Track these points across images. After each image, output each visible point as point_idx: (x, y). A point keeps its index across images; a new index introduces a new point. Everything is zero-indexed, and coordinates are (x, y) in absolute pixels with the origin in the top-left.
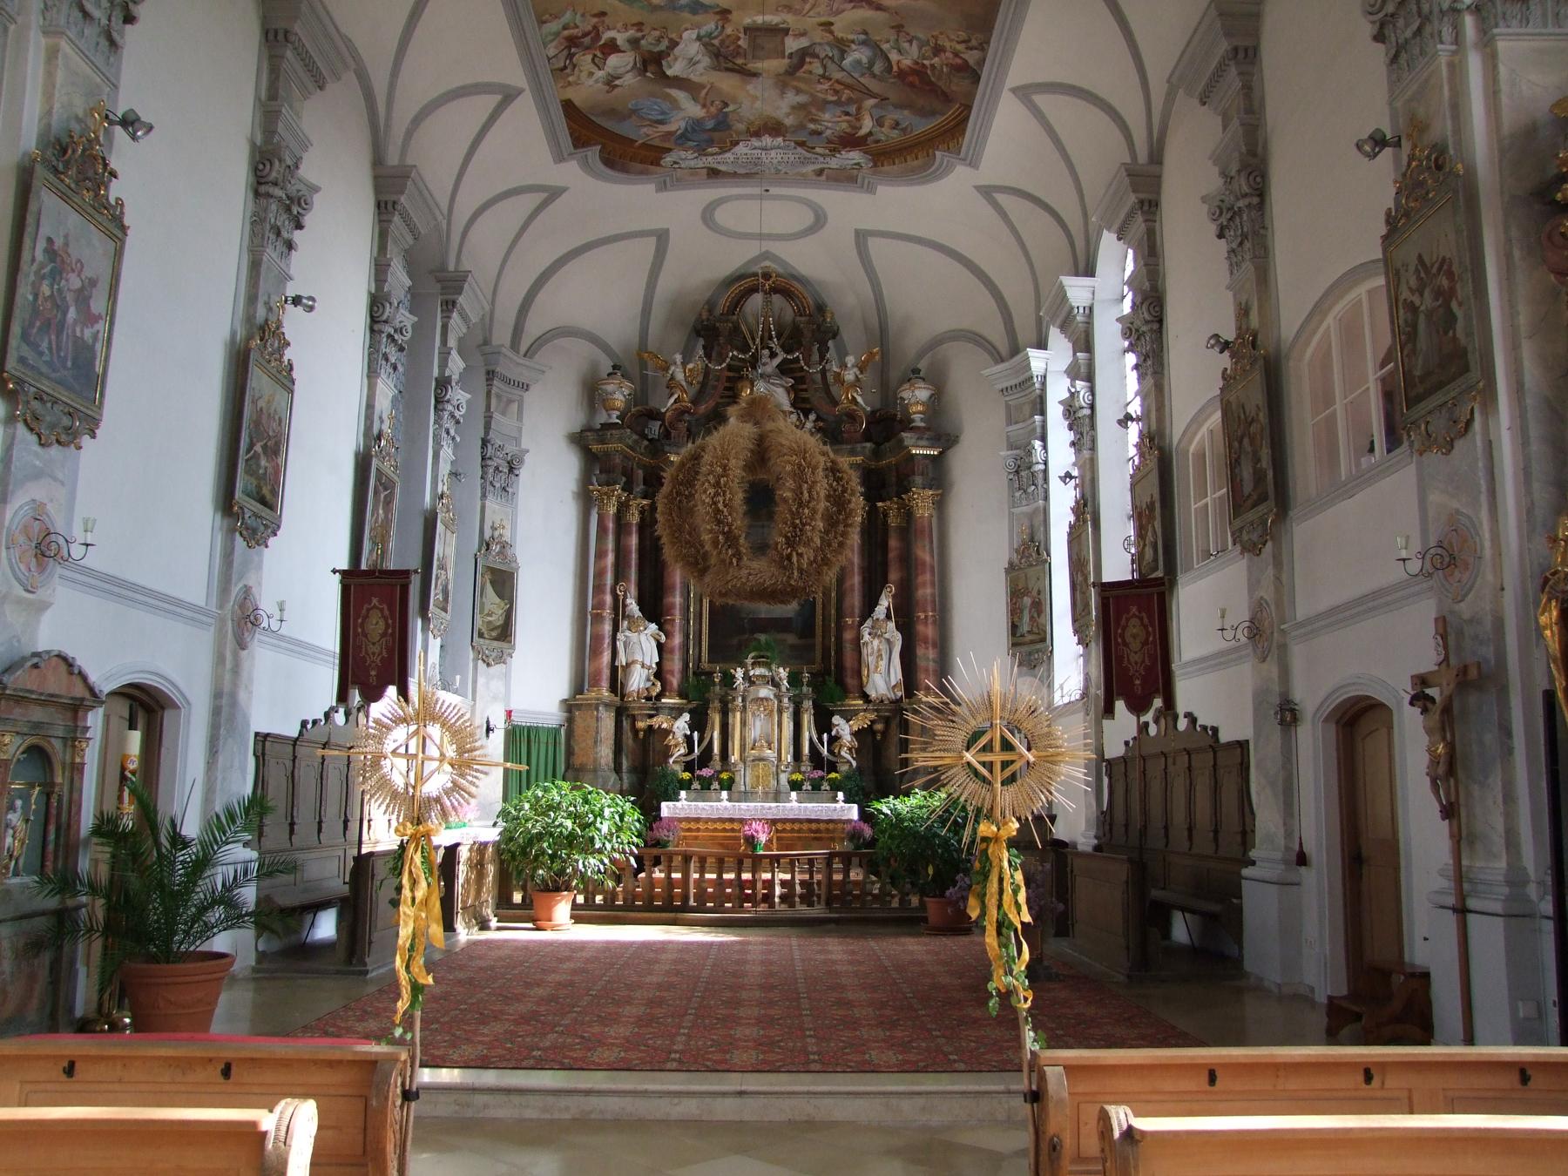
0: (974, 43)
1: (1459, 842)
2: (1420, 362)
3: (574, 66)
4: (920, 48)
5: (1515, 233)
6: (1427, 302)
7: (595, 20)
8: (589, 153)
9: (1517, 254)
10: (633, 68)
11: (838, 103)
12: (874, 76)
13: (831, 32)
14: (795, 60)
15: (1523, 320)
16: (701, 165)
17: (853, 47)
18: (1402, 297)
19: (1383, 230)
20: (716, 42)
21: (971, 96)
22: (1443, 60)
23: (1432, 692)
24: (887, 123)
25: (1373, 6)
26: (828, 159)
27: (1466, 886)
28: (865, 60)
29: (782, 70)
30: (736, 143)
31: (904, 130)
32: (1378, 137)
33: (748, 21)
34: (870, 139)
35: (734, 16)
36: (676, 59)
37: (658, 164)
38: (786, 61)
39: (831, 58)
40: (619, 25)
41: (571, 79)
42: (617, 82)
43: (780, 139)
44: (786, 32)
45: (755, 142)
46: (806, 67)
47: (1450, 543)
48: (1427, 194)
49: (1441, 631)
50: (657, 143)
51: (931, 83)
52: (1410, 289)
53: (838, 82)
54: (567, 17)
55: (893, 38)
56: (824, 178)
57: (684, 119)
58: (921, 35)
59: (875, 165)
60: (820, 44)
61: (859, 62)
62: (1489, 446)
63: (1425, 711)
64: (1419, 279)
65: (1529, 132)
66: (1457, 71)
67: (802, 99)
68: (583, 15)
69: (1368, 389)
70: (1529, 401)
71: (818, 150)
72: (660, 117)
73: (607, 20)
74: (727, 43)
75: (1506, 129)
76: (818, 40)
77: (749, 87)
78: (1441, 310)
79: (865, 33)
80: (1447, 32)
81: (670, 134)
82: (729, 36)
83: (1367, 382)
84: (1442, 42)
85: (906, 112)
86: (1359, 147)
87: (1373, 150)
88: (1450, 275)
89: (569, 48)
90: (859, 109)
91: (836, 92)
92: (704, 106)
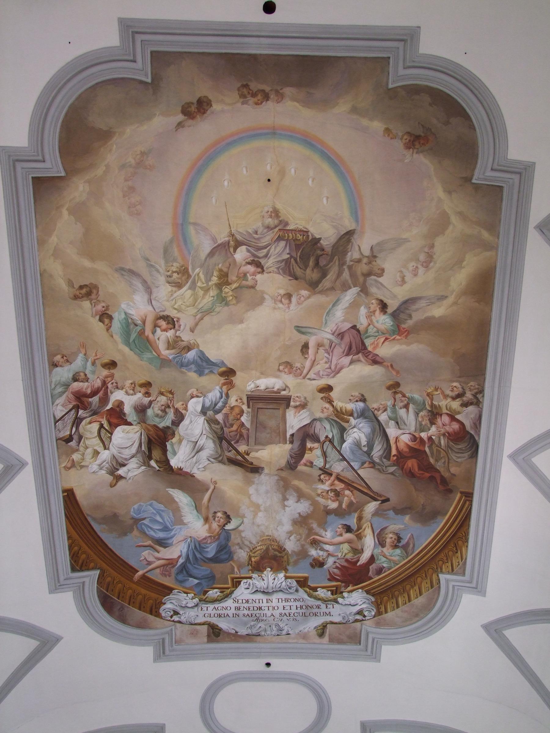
0: (469, 395)
3: (80, 438)
4: (417, 414)
7: (105, 372)
8: (87, 580)
10: (138, 452)
11: (339, 513)
12: (373, 464)
13: (330, 402)
14: (297, 444)
16: (201, 620)
17: (353, 421)
20: (220, 417)
21: (470, 478)
24: (390, 538)
26: (330, 609)
28: (364, 442)
29: (283, 463)
30: (236, 583)
31: (405, 547)
33: (251, 386)
34: (373, 567)
35: (237, 380)
36: (180, 441)
37: (158, 615)
38: (288, 446)
39: (331, 441)
40: (128, 383)
41: (76, 457)
42: (121, 472)
43: (281, 575)
44: (287, 400)
45: (257, 582)
46: (307, 456)
50: (156, 576)
51: (430, 468)
53: (339, 478)
54: (78, 363)
55: (390, 403)
56: (326, 638)
57: (185, 539)
58: (416, 396)
59: (379, 613)
60: (320, 420)
61: (358, 444)
67: (303, 507)
68: (93, 364)
71: (321, 593)
72: (161, 535)
73: (117, 373)
74: (231, 418)
76: (318, 415)
77: (252, 490)
79: (363, 399)
81: (171, 563)
82: (232, 408)
85: (407, 518)
89: (77, 408)
90: (360, 518)
91: (337, 494)
92: (206, 520)
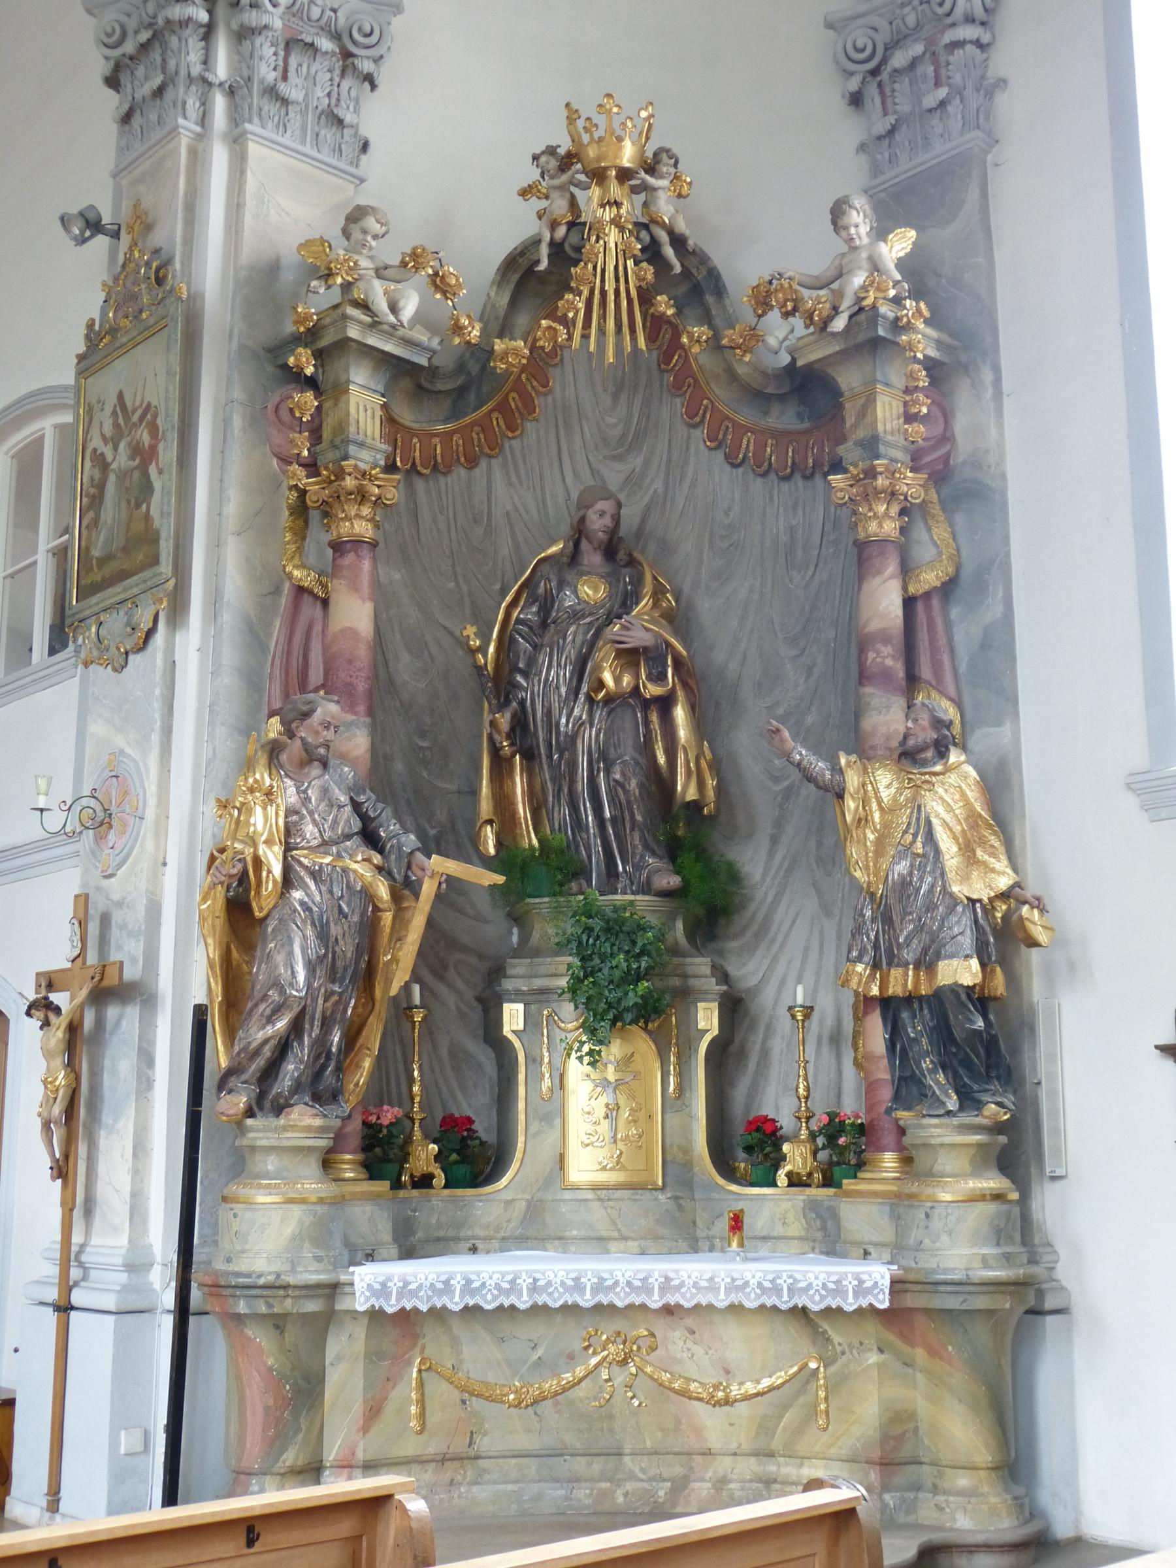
1: (71, 1210)
2: (102, 539)
5: (237, 393)
6: (121, 460)
9: (237, 422)
15: (232, 509)
18: (91, 446)
19: (82, 348)
22: (184, 142)
23: (59, 998)
25: (109, 35)
27: (75, 1273)
32: (91, 216)
47: (108, 794)
48: (141, 312)
49: (81, 915)
52: (103, 436)
62: (171, 666)
63: (46, 1024)
64: (116, 425)
65: (273, 269)
66: (199, 160)
69: (35, 563)
70: (228, 618)
75: (245, 257)
78: (136, 474)
80: (193, 104)
83: (35, 552)
84: (185, 118)
86: (65, 221)
87: (82, 232)
88: (154, 429)
